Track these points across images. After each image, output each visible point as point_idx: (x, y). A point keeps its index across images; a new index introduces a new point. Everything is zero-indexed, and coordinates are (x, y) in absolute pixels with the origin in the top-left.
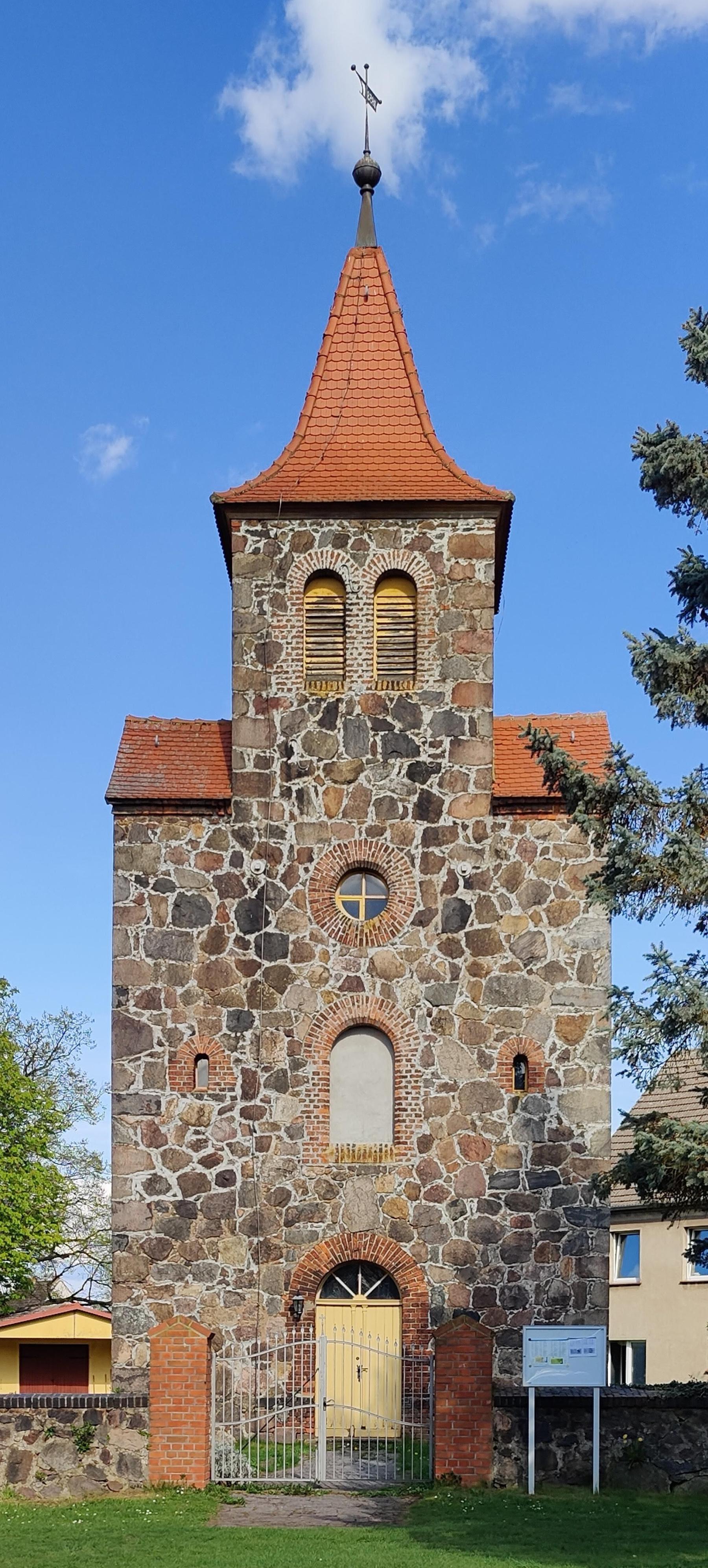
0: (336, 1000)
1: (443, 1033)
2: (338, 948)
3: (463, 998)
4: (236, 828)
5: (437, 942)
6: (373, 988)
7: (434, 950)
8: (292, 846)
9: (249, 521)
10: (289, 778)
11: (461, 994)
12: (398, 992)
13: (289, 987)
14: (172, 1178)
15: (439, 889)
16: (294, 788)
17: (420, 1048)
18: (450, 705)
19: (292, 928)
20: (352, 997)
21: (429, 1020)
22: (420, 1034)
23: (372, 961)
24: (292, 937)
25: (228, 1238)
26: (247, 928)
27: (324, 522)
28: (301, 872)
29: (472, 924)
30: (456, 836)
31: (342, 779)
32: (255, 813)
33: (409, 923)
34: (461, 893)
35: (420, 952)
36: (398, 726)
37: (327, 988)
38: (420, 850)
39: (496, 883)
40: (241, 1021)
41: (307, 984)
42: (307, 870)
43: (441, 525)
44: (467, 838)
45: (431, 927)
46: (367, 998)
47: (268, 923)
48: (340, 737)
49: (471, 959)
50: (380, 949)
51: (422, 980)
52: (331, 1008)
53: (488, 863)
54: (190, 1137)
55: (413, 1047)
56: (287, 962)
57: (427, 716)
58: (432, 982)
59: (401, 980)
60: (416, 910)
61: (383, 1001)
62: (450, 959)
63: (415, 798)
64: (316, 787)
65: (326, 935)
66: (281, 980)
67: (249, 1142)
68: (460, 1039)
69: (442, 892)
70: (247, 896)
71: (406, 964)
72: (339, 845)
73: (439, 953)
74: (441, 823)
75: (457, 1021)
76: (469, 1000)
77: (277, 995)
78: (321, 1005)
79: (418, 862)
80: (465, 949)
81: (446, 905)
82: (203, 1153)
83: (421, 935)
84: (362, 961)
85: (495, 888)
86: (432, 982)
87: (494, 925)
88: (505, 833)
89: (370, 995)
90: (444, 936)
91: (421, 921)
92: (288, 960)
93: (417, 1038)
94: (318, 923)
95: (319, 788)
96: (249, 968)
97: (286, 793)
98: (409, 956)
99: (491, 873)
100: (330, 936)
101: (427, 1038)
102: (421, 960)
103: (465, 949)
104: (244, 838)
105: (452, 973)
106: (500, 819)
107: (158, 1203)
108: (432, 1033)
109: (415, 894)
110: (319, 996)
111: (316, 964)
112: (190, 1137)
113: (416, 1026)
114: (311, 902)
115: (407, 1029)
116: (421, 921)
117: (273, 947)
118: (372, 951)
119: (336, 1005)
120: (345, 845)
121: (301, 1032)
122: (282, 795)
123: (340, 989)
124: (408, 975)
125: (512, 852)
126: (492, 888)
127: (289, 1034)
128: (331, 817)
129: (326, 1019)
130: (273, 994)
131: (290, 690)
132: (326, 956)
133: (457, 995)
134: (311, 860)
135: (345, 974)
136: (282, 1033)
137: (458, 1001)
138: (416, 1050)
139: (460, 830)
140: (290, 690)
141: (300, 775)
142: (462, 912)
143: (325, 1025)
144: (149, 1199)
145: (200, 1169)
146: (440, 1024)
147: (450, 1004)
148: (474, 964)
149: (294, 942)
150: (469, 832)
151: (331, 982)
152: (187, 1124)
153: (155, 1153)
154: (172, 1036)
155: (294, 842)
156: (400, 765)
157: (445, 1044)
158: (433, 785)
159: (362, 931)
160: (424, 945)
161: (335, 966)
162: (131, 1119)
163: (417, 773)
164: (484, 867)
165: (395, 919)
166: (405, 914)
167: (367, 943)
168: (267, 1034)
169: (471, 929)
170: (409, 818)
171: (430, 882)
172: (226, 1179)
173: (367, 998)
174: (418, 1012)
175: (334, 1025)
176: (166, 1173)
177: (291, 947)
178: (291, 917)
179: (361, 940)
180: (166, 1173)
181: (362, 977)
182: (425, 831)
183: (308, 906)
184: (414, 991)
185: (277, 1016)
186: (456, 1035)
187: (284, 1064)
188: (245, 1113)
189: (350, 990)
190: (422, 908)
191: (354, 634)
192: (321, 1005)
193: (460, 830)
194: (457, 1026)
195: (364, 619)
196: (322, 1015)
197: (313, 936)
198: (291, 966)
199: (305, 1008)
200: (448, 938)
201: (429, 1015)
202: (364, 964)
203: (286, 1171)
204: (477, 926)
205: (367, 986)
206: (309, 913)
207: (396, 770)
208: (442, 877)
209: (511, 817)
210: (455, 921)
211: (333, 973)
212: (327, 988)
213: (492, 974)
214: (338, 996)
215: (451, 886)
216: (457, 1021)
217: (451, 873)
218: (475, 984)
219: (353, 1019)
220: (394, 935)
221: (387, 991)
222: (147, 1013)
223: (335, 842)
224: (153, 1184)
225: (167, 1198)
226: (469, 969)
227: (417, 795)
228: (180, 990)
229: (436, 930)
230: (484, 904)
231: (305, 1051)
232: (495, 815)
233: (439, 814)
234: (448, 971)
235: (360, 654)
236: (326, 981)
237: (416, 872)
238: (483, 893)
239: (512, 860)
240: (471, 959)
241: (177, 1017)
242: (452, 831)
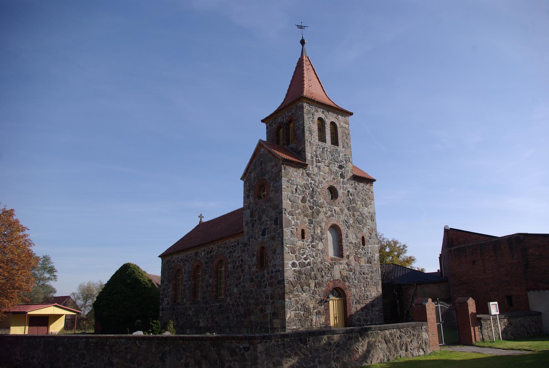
10: (317, 163)
14: (297, 263)
25: (311, 281)
40: (311, 222)
54: (301, 252)
57: (341, 155)
66: (318, 212)
67: (314, 255)
82: (305, 256)
96: (312, 208)
97: (316, 166)
104: (308, 175)
107: (294, 270)
111: (324, 209)
112: (301, 252)
117: (315, 203)
141: (319, 162)
144: (293, 269)
145: (304, 261)
152: (301, 248)
153: (294, 255)
154: (296, 224)
156: (337, 165)
162: (288, 246)
163: (341, 167)
172: (309, 264)
176: (296, 262)
180: (296, 262)
187: (320, 234)
188: (313, 246)
203: (322, 263)
222: (290, 217)
224: (294, 265)
225: (297, 269)
228: (297, 212)
241: (297, 219)
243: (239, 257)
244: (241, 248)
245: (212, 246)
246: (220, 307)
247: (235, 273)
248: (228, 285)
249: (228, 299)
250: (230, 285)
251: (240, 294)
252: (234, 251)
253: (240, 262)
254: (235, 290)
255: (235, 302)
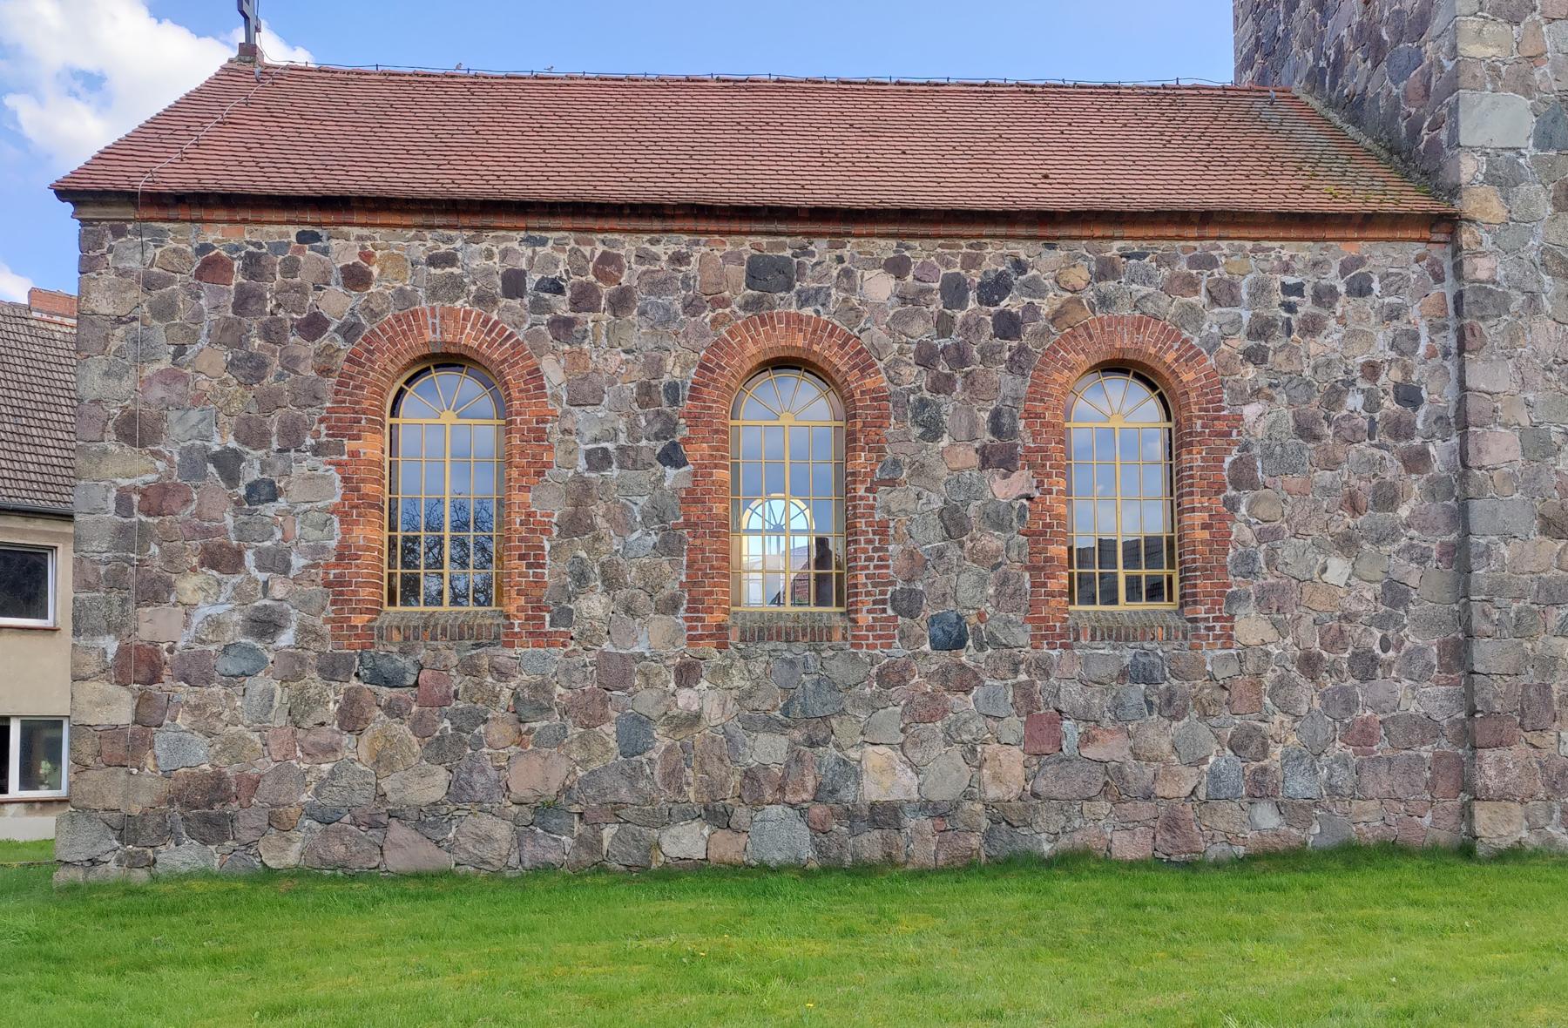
243: (1372, 370)
244: (1394, 314)
245: (1022, 250)
246: (1140, 673)
247: (1332, 464)
248: (1241, 531)
249: (1251, 627)
250: (1269, 535)
251: (1395, 593)
252: (1312, 327)
253: (1389, 405)
254: (1338, 569)
255: (1336, 640)
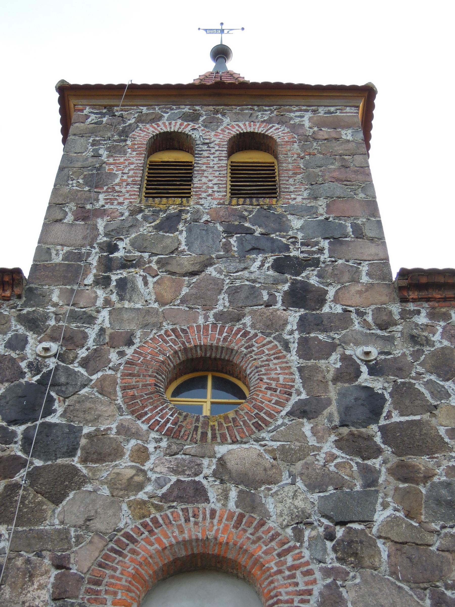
0: (154, 513)
1: (359, 565)
2: (164, 444)
3: (389, 512)
4: (25, 312)
5: (333, 438)
6: (223, 500)
7: (329, 446)
8: (102, 331)
9: (93, 106)
11: (385, 506)
12: (270, 505)
13: (71, 495)
15: (330, 376)
16: (114, 278)
17: (316, 589)
18: (325, 216)
19: (89, 417)
20: (185, 511)
21: (329, 545)
22: (315, 567)
23: (222, 462)
24: (86, 430)
26: (13, 416)
27: (174, 107)
28: (113, 356)
29: (389, 416)
30: (351, 322)
31: (184, 271)
32: (55, 298)
33: (283, 413)
34: (365, 378)
35: (305, 451)
36: (258, 231)
37: (141, 495)
38: (297, 335)
39: (420, 369)
41: (105, 491)
42: (122, 354)
43: (301, 110)
44: (365, 324)
45: (323, 421)
46: (213, 512)
47: (49, 411)
48: (183, 238)
49: (394, 460)
50: (234, 447)
51: (312, 488)
52: (145, 525)
53: (401, 349)
55: (302, 587)
56: (76, 461)
58: (331, 490)
59: (275, 488)
60: (294, 399)
61: (241, 516)
62: (359, 460)
63: (286, 287)
64: (144, 278)
65: (145, 427)
68: (393, 573)
69: (335, 380)
70: (23, 381)
71: (282, 465)
72: (174, 330)
73: (336, 451)
74: (326, 309)
75: (384, 549)
76: (401, 514)
77: (48, 506)
78: (126, 520)
79: (294, 347)
80: (383, 446)
81: (342, 395)
83: (307, 428)
84: (205, 462)
85: (419, 374)
86: (331, 490)
87: (426, 416)
88: (422, 319)
89: (218, 506)
90: (345, 431)
91: (303, 411)
92: (76, 459)
93: (309, 573)
94: (132, 413)
95: (150, 279)
98: (287, 456)
99: (410, 359)
100: (151, 428)
101: (327, 572)
102: (310, 459)
103: (383, 446)
105: (364, 477)
106: (411, 307)
108: (337, 565)
109: (293, 380)
110: (125, 507)
111: (125, 466)
113: (307, 554)
114: (124, 389)
115: (289, 560)
116: (303, 411)
118: (221, 450)
119: (155, 521)
120: (183, 331)
121: (82, 560)
122: (97, 282)
123: (164, 498)
124: (286, 479)
125: (437, 337)
126: (413, 374)
127: (61, 564)
128: (162, 304)
129: (133, 540)
130: (41, 503)
131: (120, 204)
132: (142, 454)
133: (379, 507)
134: (130, 343)
135: (174, 479)
136: (47, 561)
137: (380, 516)
138: (309, 592)
139: (354, 316)
140: (120, 204)
142: (373, 404)
143: (133, 552)
146: (353, 552)
147: (368, 522)
148: (401, 466)
149: (89, 436)
150: (369, 319)
151: (149, 488)
155: (107, 324)
157: (365, 581)
158: (312, 277)
159: (206, 424)
160: (312, 441)
161: (158, 466)
164: (398, 353)
165: (261, 409)
166: (277, 403)
167: (214, 437)
168: (19, 562)
169: (387, 422)
170: (279, 305)
171: (316, 368)
173: (213, 512)
174: (307, 533)
175: (150, 549)
177: (83, 441)
178: (88, 405)
179: (204, 434)
181: (204, 482)
182: (302, 318)
183: (119, 394)
184: (299, 503)
185: (41, 536)
186: (384, 567)
189: (180, 499)
190: (304, 396)
191: (204, 167)
192: (126, 520)
193: (354, 316)
194: (384, 555)
195: (216, 159)
196: (127, 536)
197: (121, 429)
198: (79, 466)
199: (97, 525)
200: (351, 434)
201: (330, 536)
202: (208, 466)
204: (396, 418)
205: (212, 495)
206: (120, 401)
207: (258, 263)
208: (334, 362)
209: (426, 305)
210: (361, 413)
211: (153, 477)
212: (141, 495)
213: (436, 479)
214: (158, 508)
215: (349, 370)
216: (384, 549)
217: (345, 358)
218: (407, 492)
219: (185, 543)
220: (259, 428)
221: (250, 503)
223: (167, 326)
226: (391, 471)
227: (289, 284)
229: (330, 421)
230: (405, 395)
231: (88, 591)
232: (404, 300)
233: (322, 301)
234: (356, 475)
235: (211, 181)
236: (140, 487)
237: (293, 358)
238: (399, 380)
239: (438, 345)
240: (394, 460)
242: (344, 319)
